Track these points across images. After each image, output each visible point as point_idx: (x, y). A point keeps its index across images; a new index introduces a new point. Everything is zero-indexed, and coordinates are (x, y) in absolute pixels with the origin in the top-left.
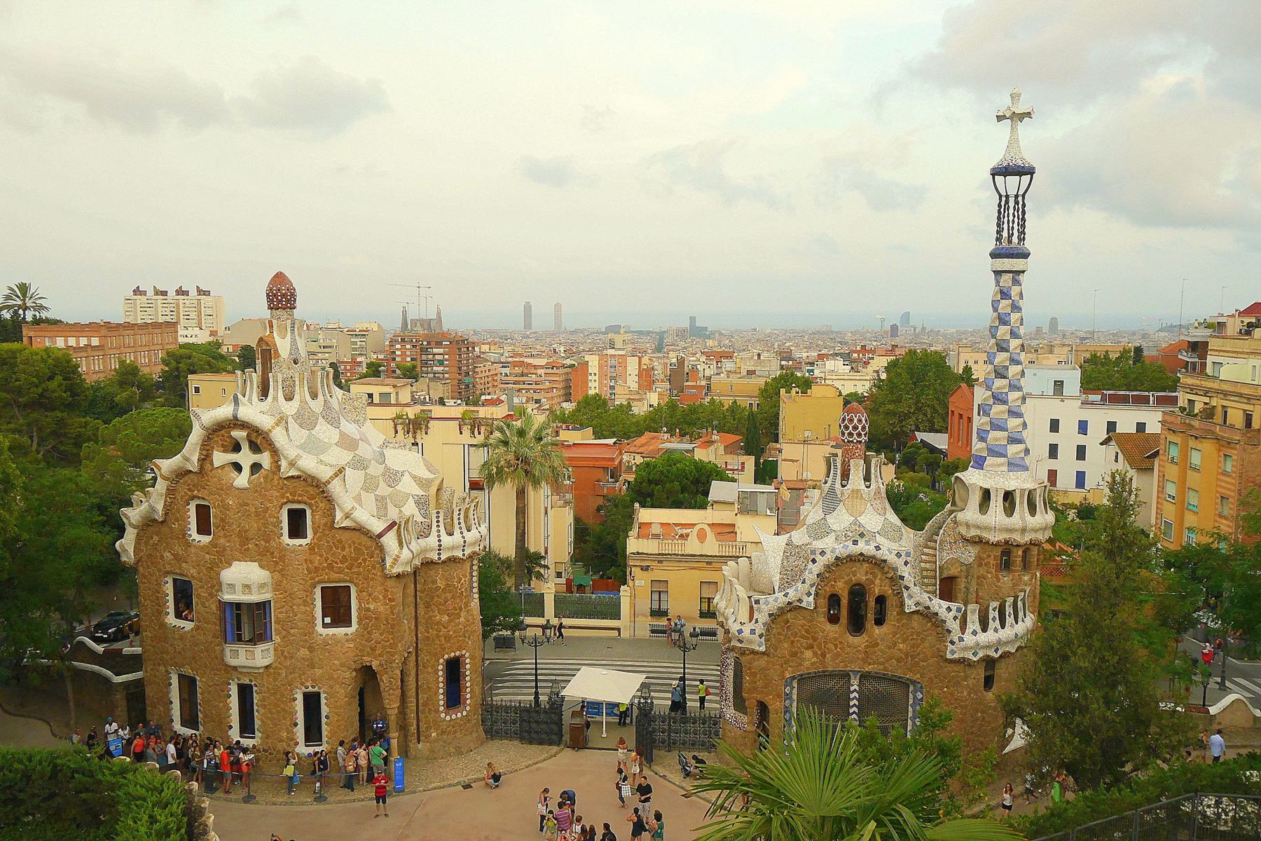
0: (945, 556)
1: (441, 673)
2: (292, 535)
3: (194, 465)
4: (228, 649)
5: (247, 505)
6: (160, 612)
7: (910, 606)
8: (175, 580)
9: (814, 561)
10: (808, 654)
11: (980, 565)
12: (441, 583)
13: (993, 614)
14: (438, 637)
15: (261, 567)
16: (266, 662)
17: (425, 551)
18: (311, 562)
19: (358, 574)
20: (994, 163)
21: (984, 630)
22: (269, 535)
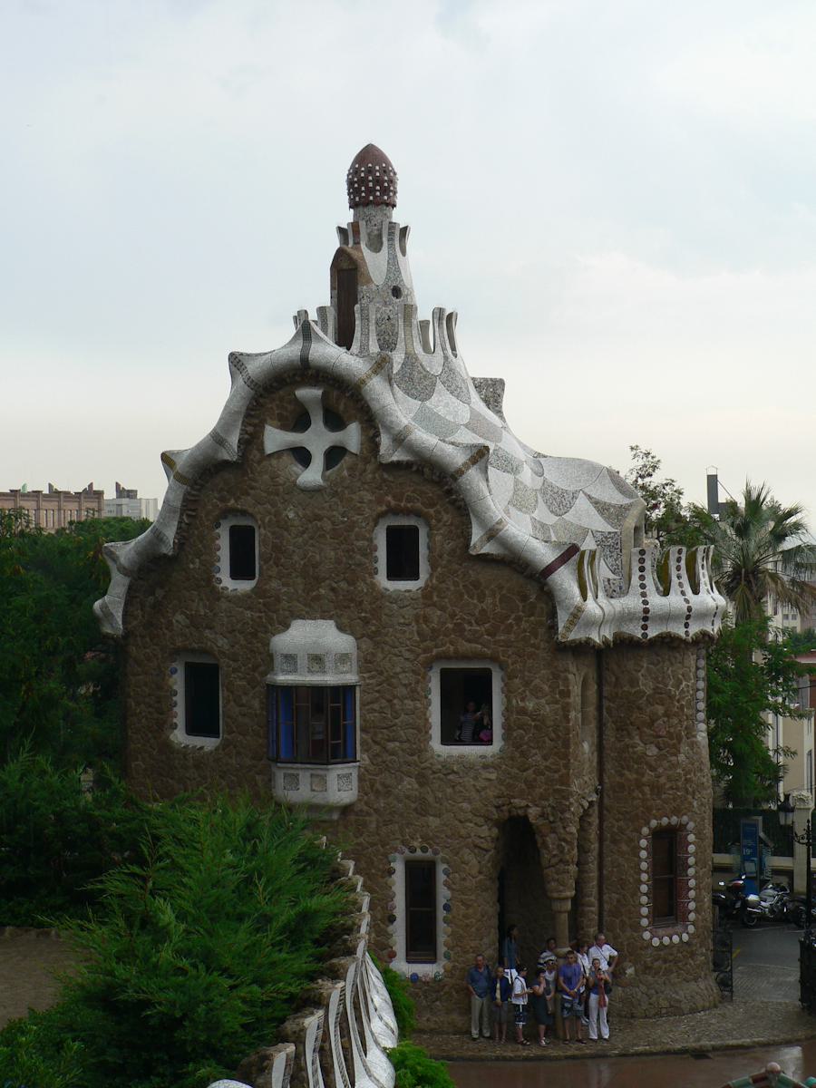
1: (643, 854)
2: (393, 575)
3: (231, 452)
5: (318, 518)
12: (646, 685)
14: (639, 785)
15: (341, 628)
18: (426, 619)
19: (508, 644)
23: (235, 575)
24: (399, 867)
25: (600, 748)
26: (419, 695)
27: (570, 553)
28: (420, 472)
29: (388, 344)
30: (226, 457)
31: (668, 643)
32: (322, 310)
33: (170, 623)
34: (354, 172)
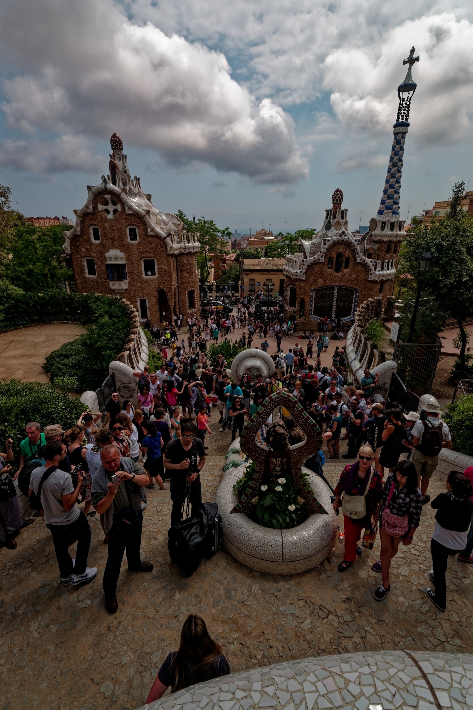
0: (367, 247)
2: (131, 239)
3: (90, 210)
4: (111, 283)
5: (113, 226)
6: (83, 272)
7: (358, 260)
8: (87, 260)
9: (325, 244)
10: (320, 280)
11: (379, 251)
12: (186, 262)
13: (386, 265)
15: (121, 251)
16: (126, 287)
17: (181, 248)
19: (157, 254)
20: (401, 81)
21: (382, 270)
22: (122, 238)
23: (95, 239)
24: (138, 301)
25: (177, 275)
26: (139, 265)
27: (169, 234)
28: (135, 216)
29: (125, 185)
30: (89, 211)
31: (190, 254)
32: (108, 176)
33: (81, 251)
34: (112, 140)
